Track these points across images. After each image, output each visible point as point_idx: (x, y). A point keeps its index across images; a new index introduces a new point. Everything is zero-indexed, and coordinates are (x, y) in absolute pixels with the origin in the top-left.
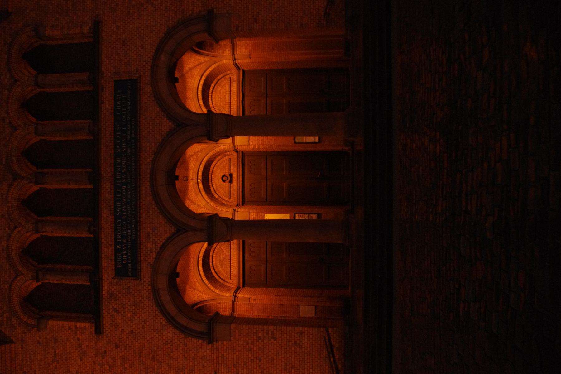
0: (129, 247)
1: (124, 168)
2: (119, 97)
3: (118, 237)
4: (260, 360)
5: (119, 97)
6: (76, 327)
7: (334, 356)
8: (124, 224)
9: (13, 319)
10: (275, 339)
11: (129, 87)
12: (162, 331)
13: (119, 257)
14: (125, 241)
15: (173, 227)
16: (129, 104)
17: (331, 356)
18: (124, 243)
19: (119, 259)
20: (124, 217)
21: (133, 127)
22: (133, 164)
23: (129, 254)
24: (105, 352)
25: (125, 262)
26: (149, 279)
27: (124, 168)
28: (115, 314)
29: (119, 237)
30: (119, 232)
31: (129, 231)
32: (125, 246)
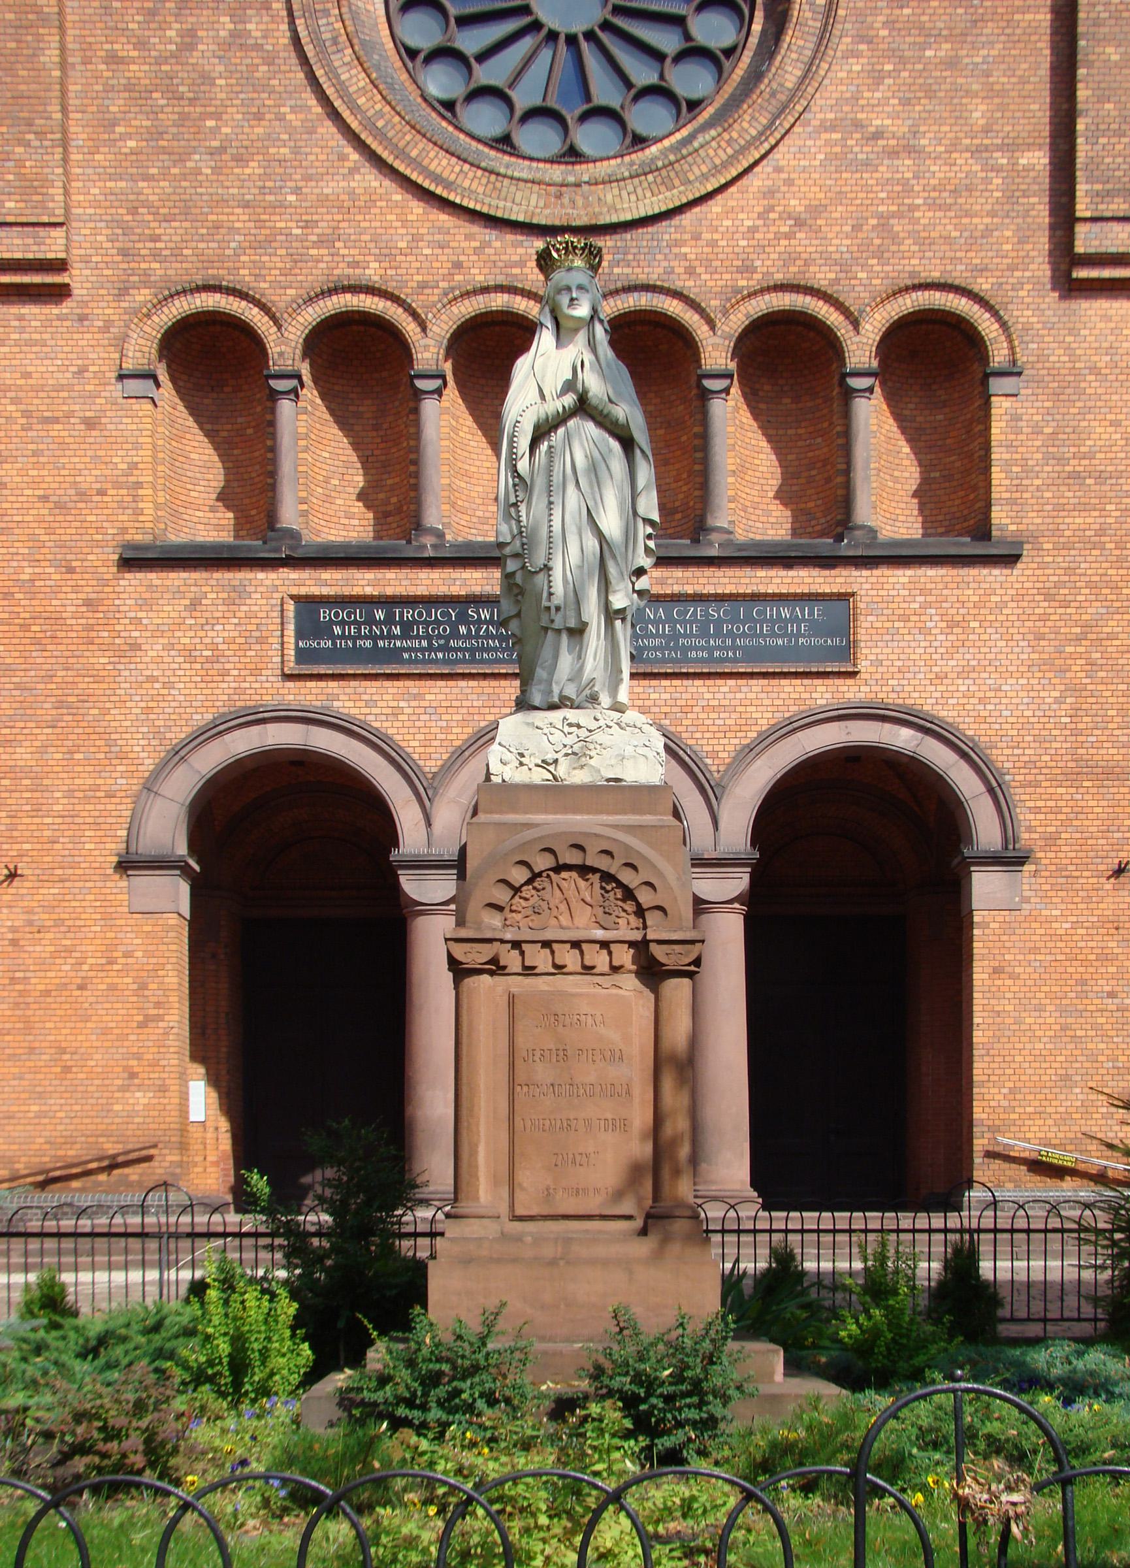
0: (381, 643)
4: (81, 987)
6: (139, 485)
7: (101, 1170)
8: (445, 630)
9: (147, 291)
10: (142, 1025)
12: (145, 730)
14: (397, 631)
15: (439, 763)
16: (780, 642)
17: (105, 1163)
18: (390, 630)
19: (343, 615)
20: (463, 630)
21: (716, 654)
24: (71, 570)
25: (337, 630)
26: (291, 697)
28: (188, 602)
29: (408, 615)
31: (425, 643)
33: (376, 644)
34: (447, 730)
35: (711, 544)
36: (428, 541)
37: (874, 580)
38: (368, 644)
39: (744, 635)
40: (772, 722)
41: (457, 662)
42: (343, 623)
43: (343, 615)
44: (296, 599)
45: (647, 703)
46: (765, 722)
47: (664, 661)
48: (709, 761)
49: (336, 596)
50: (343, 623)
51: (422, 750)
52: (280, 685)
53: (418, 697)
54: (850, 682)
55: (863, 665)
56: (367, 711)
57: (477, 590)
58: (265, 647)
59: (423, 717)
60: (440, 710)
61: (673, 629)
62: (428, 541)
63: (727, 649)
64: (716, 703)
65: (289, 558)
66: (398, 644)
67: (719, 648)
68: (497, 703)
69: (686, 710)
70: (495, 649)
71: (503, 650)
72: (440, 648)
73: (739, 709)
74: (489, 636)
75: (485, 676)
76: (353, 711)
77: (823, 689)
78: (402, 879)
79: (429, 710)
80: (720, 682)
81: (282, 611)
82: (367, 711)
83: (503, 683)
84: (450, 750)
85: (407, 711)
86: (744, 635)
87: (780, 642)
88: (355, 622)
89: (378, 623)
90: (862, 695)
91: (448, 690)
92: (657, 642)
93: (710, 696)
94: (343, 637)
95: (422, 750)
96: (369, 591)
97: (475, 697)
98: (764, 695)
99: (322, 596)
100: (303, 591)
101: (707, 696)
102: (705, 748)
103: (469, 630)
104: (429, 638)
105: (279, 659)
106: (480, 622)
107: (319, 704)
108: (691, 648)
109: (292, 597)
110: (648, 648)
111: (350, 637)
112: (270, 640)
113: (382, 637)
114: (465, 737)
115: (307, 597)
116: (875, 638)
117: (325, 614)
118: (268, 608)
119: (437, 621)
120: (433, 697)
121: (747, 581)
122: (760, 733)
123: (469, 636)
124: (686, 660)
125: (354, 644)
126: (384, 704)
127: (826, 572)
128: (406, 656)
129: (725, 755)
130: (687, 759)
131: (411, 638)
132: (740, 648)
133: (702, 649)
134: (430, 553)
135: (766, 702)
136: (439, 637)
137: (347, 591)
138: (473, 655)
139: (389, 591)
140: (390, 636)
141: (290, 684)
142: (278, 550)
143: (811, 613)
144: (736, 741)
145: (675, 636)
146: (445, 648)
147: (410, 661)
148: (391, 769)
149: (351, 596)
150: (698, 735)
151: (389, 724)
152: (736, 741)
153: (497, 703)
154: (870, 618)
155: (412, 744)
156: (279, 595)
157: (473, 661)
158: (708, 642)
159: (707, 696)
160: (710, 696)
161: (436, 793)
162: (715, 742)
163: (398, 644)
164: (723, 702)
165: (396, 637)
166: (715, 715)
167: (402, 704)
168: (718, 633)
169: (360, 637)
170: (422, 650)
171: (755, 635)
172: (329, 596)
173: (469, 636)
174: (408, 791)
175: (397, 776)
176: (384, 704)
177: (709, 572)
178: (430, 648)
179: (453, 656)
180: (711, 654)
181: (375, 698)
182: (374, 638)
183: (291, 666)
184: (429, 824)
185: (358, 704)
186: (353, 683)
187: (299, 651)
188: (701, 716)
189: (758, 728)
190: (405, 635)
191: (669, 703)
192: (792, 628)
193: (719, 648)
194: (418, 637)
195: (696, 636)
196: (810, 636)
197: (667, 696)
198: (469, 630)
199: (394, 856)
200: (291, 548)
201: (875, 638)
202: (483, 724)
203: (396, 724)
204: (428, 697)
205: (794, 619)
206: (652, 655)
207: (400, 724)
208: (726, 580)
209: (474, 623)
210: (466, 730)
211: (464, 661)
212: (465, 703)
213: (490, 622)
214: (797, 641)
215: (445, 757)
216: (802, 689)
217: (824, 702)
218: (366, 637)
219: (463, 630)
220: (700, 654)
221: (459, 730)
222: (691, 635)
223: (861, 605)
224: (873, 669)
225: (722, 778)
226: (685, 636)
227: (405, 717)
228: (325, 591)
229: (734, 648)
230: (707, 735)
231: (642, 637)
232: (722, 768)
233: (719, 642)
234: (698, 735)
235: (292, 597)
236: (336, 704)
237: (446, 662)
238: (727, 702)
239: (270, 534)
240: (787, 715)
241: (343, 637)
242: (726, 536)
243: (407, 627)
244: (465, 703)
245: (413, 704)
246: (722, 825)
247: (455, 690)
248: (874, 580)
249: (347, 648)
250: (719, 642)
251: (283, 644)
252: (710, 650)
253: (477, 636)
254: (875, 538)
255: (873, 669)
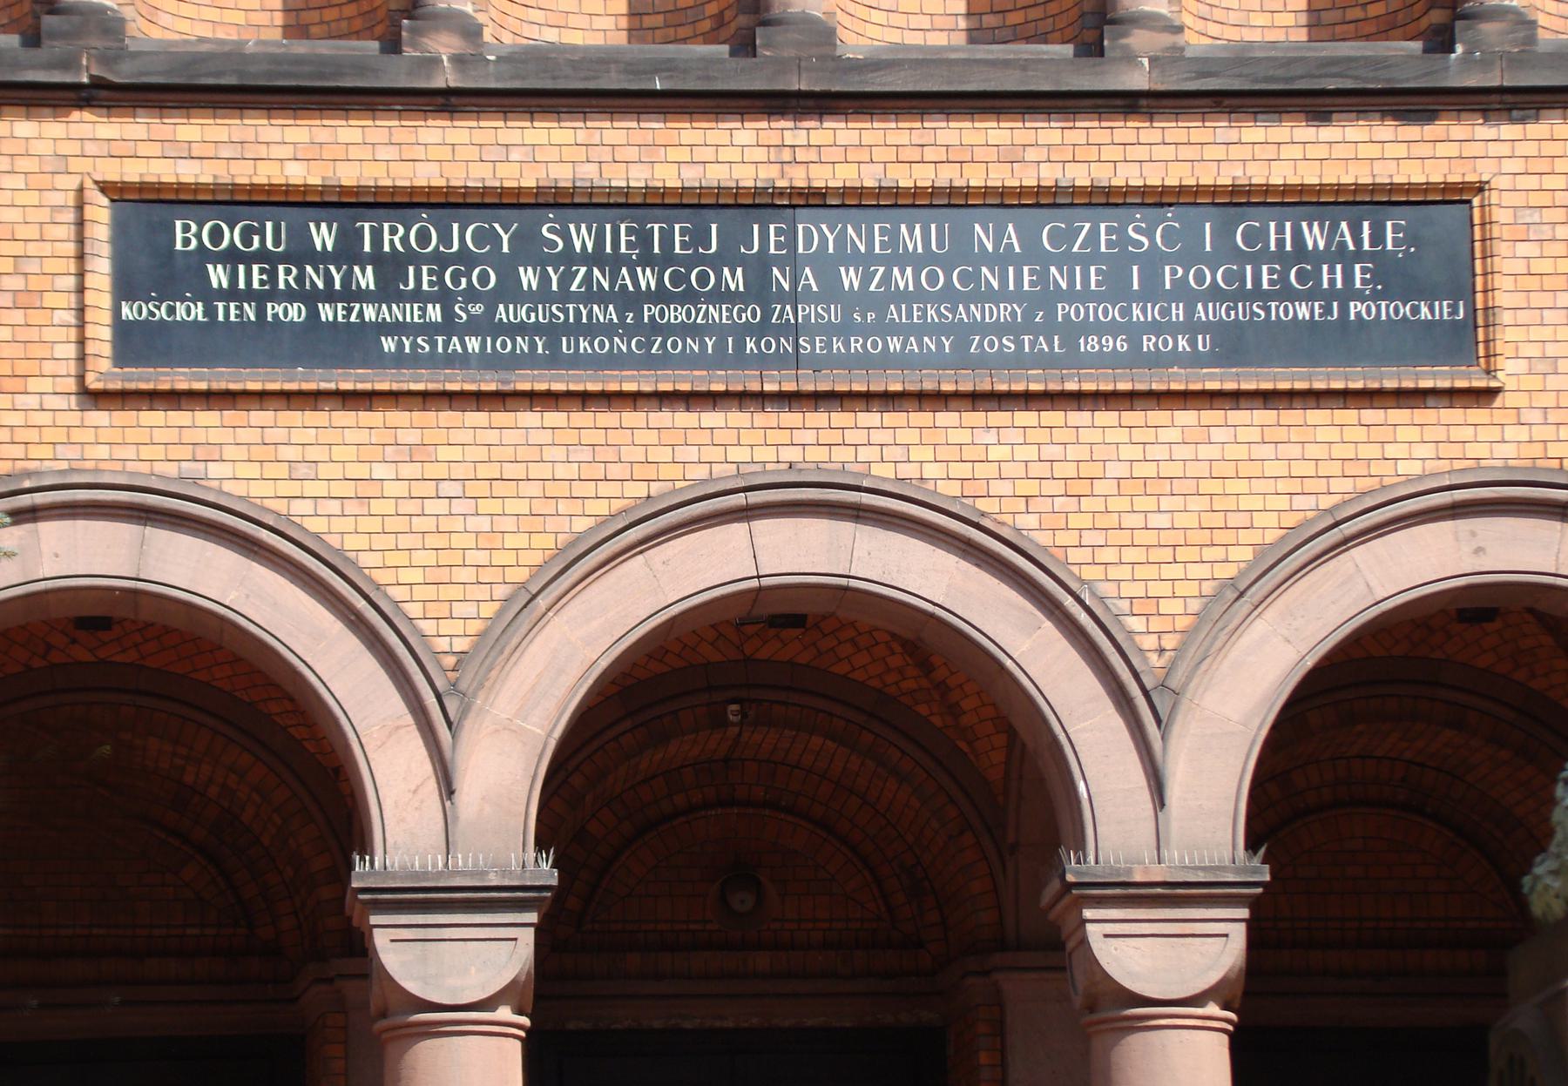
1: (866, 279)
2: (1358, 241)
3: (393, 231)
5: (1358, 241)
8: (484, 278)
11: (1424, 310)
13: (247, 240)
14: (366, 278)
15: (475, 627)
16: (1303, 312)
18: (347, 278)
19: (232, 236)
20: (528, 278)
21: (1148, 343)
22: (895, 344)
23: (273, 309)
25: (218, 276)
26: (103, 452)
27: (866, 279)
29: (392, 239)
30: (423, 238)
32: (329, 280)
33: (314, 314)
34: (490, 540)
35: (1130, 58)
36: (444, 45)
37: (1530, 149)
38: (295, 312)
39: (1215, 294)
40: (1290, 520)
41: (514, 362)
42: (232, 258)
43: (232, 236)
44: (116, 192)
45: (982, 471)
46: (1270, 520)
47: (1019, 361)
48: (1136, 624)
49: (216, 187)
50: (232, 258)
51: (429, 592)
52: (74, 418)
53: (416, 452)
54: (1477, 415)
55: (1509, 371)
56: (292, 488)
57: (562, 175)
58: (36, 317)
59: (432, 507)
60: (474, 489)
61: (1042, 277)
62: (444, 45)
63: (1174, 329)
64: (1149, 470)
65: (98, 84)
66: (370, 313)
67: (1156, 328)
68: (615, 471)
69: (1078, 487)
70: (609, 330)
71: (629, 332)
72: (474, 327)
73: (1208, 486)
74: (592, 295)
75: (584, 399)
76: (257, 489)
77: (1413, 434)
78: (381, 939)
79: (448, 489)
80: (1158, 416)
81: (80, 223)
82: (292, 488)
83: (632, 418)
84: (501, 592)
85: (393, 489)
86: (1215, 294)
87: (1303, 312)
88: (263, 256)
89: (319, 259)
90: (1508, 451)
91: (493, 437)
92: (1003, 312)
93: (1136, 452)
94: (232, 294)
95: (429, 592)
96: (296, 174)
97: (558, 453)
98: (1267, 451)
99: (181, 187)
100: (133, 172)
101: (1128, 452)
102: (1128, 590)
103: (545, 280)
104: (444, 297)
105: (71, 351)
106: (569, 258)
107: (171, 470)
108: (1086, 328)
109: (105, 187)
110: (983, 329)
111: (249, 295)
112: (50, 300)
113: (330, 296)
114: (537, 558)
115: (142, 187)
116: (1538, 300)
117: (186, 234)
118: (44, 215)
119: (466, 259)
120: (454, 453)
121: (1218, 152)
122: (1261, 550)
123: (542, 295)
124: (1074, 360)
125: (261, 312)
126: (335, 471)
127: (1412, 131)
128: (389, 344)
129: (1175, 607)
130: (1083, 618)
131: (401, 298)
132: (1206, 327)
133: (1113, 329)
134: (447, 77)
135: (1273, 469)
136: (471, 295)
137: (243, 174)
138: (553, 345)
139: (348, 176)
140: (351, 295)
141: (99, 417)
142: (69, 64)
143: (1378, 237)
144: (1202, 571)
145: (1046, 297)
146: (485, 327)
147: (399, 360)
148: (352, 643)
149: (254, 188)
150: (1108, 555)
151: (347, 524)
152: (1202, 571)
153: (615, 471)
154: (1523, 249)
155: (407, 576)
156: (73, 182)
157: (554, 360)
158: (1126, 312)
159: (1128, 452)
160: (1136, 452)
161: (465, 711)
162: (1151, 572)
163: (370, 313)
164: (1168, 470)
165: (362, 296)
166: (1148, 503)
167: (380, 471)
168: (1153, 290)
169: (273, 294)
170: (429, 329)
171: (1241, 295)
172: (197, 188)
173: (542, 295)
174: (394, 703)
175: (369, 663)
176: (335, 471)
177: (1126, 130)
178: (448, 326)
179: (503, 345)
180: (1135, 344)
181: (313, 453)
182: (310, 298)
183: (103, 371)
184: (447, 787)
185: (272, 470)
186: (259, 417)
187: (124, 332)
188: (1116, 504)
189: (1255, 537)
190: (387, 292)
191: (1037, 470)
192: (1331, 276)
193: (1156, 328)
194: (418, 296)
195: (1098, 298)
196: (1376, 296)
197: (1030, 453)
198: (545, 280)
199: (362, 874)
200: (106, 60)
201: (1538, 300)
202: (581, 525)
203: (367, 524)
204: (444, 453)
205: (1339, 255)
206: (992, 345)
207: (374, 524)
208: (1167, 152)
209: (556, 261)
210: (538, 541)
211: (529, 360)
212: (536, 471)
213: (596, 258)
214: (1344, 310)
215: (488, 610)
216: (1360, 434)
217: (1415, 468)
218: (290, 296)
219: (528, 278)
220: (1109, 343)
221: (521, 541)
222: (1085, 296)
223: (1500, 215)
224: (1534, 383)
225: (1170, 670)
226: (1071, 296)
227: (387, 507)
228: (189, 173)
229: (1192, 328)
230: (1130, 555)
231: (967, 299)
232: (1169, 642)
233: (1154, 313)
234: (1108, 555)
235: (105, 187)
236: (215, 470)
237: (490, 361)
238: (1174, 470)
239: (49, 21)
240: (1326, 502)
241: (232, 294)
242: (1166, 39)
243: (391, 267)
244: (536, 471)
245: (408, 470)
246: (1174, 792)
247: (511, 436)
248: (1530, 149)
249: (243, 324)
250: (1154, 313)
251: (81, 310)
252: (1134, 332)
253: (564, 296)
254: (1531, 39)
255: (1534, 383)
